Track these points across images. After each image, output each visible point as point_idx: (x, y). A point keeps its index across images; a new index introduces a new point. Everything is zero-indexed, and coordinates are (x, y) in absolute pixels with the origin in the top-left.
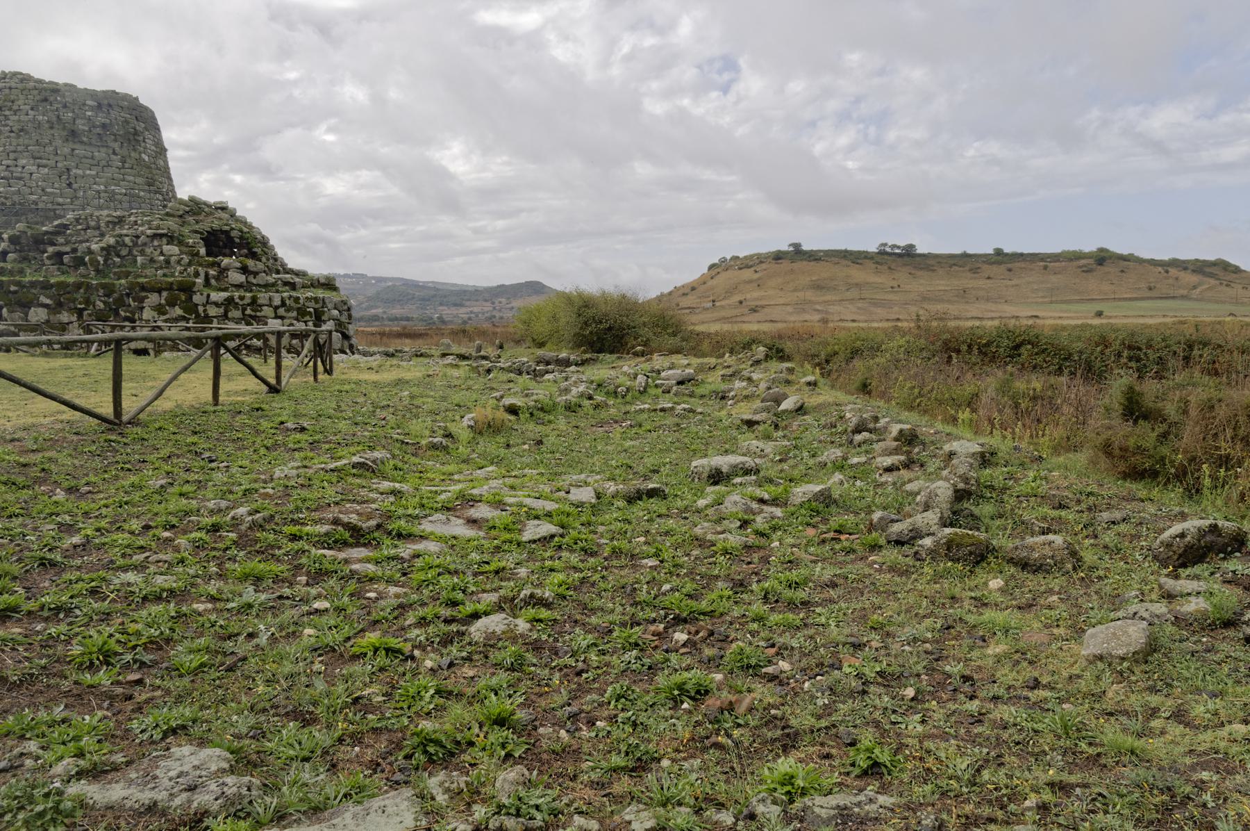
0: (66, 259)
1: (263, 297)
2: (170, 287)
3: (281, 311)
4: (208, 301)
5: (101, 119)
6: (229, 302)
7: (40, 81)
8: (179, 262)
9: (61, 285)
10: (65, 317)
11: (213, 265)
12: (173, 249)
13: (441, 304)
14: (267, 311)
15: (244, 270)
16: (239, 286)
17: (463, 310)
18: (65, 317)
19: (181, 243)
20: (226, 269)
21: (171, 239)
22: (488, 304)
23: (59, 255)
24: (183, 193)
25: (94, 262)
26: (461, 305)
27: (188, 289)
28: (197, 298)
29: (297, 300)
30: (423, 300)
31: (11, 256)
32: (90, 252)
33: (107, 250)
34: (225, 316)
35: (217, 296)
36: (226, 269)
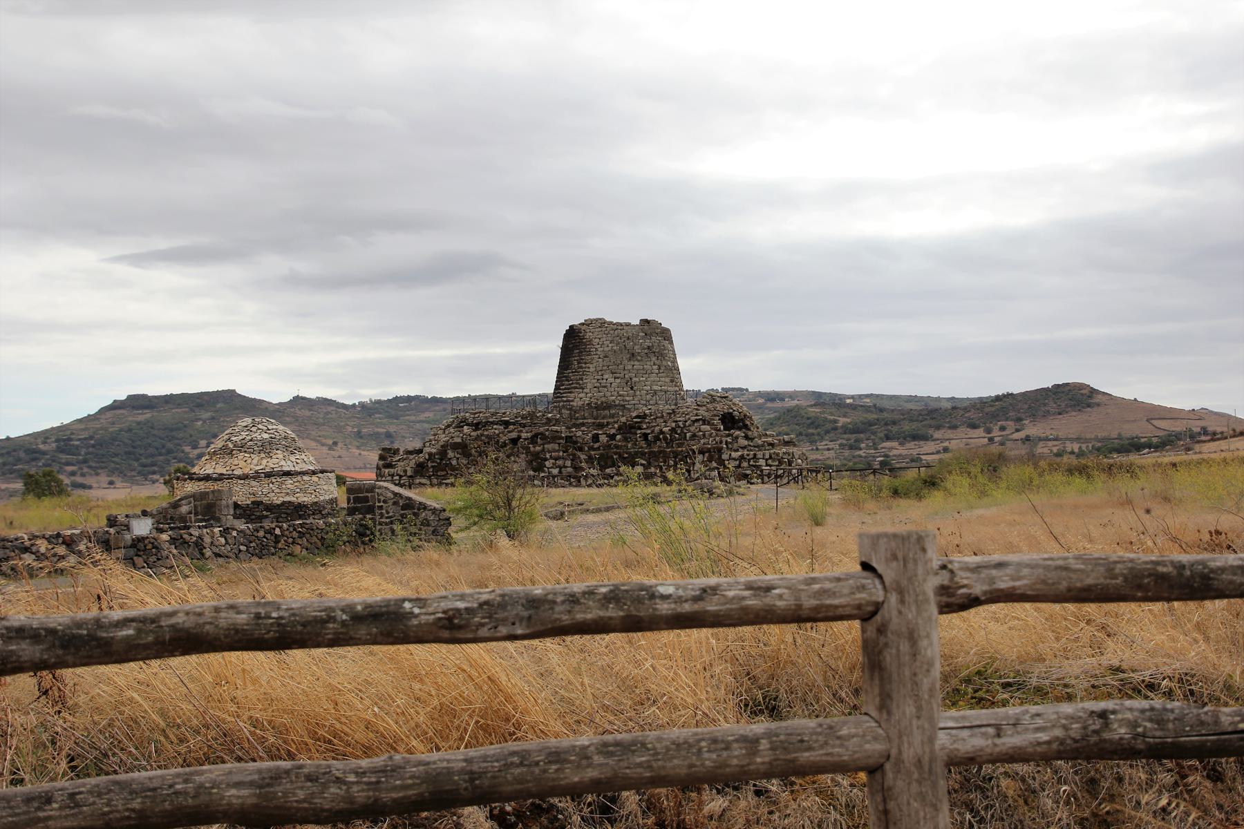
0: (650, 437)
1: (760, 454)
2: (709, 451)
3: (770, 462)
4: (730, 458)
5: (648, 343)
6: (742, 457)
7: (611, 323)
8: (711, 435)
9: (650, 453)
10: (653, 470)
11: (728, 435)
12: (708, 427)
13: (888, 438)
14: (762, 462)
15: (746, 437)
16: (744, 448)
17: (929, 447)
18: (653, 470)
19: (709, 424)
20: (737, 438)
21: (704, 422)
22: (980, 432)
23: (645, 436)
24: (688, 384)
25: (665, 438)
26: (925, 438)
27: (720, 450)
28: (725, 456)
29: (778, 454)
30: (856, 430)
31: (618, 437)
32: (661, 432)
33: (673, 430)
34: (739, 466)
35: (734, 455)
36: (737, 438)
